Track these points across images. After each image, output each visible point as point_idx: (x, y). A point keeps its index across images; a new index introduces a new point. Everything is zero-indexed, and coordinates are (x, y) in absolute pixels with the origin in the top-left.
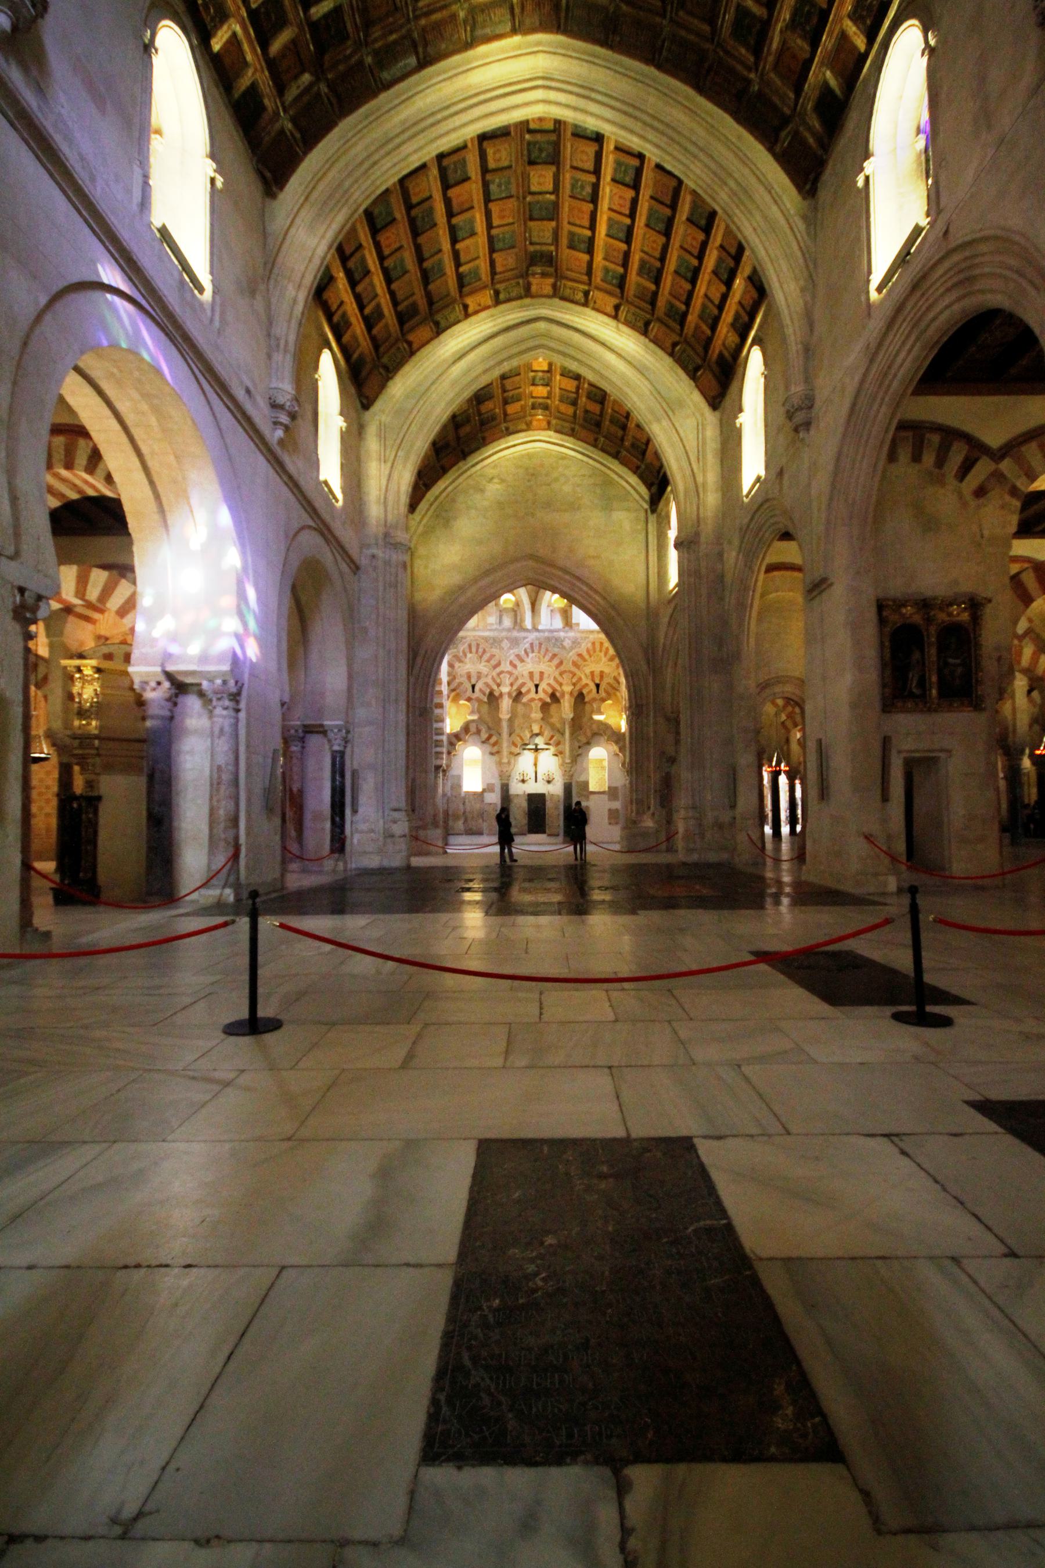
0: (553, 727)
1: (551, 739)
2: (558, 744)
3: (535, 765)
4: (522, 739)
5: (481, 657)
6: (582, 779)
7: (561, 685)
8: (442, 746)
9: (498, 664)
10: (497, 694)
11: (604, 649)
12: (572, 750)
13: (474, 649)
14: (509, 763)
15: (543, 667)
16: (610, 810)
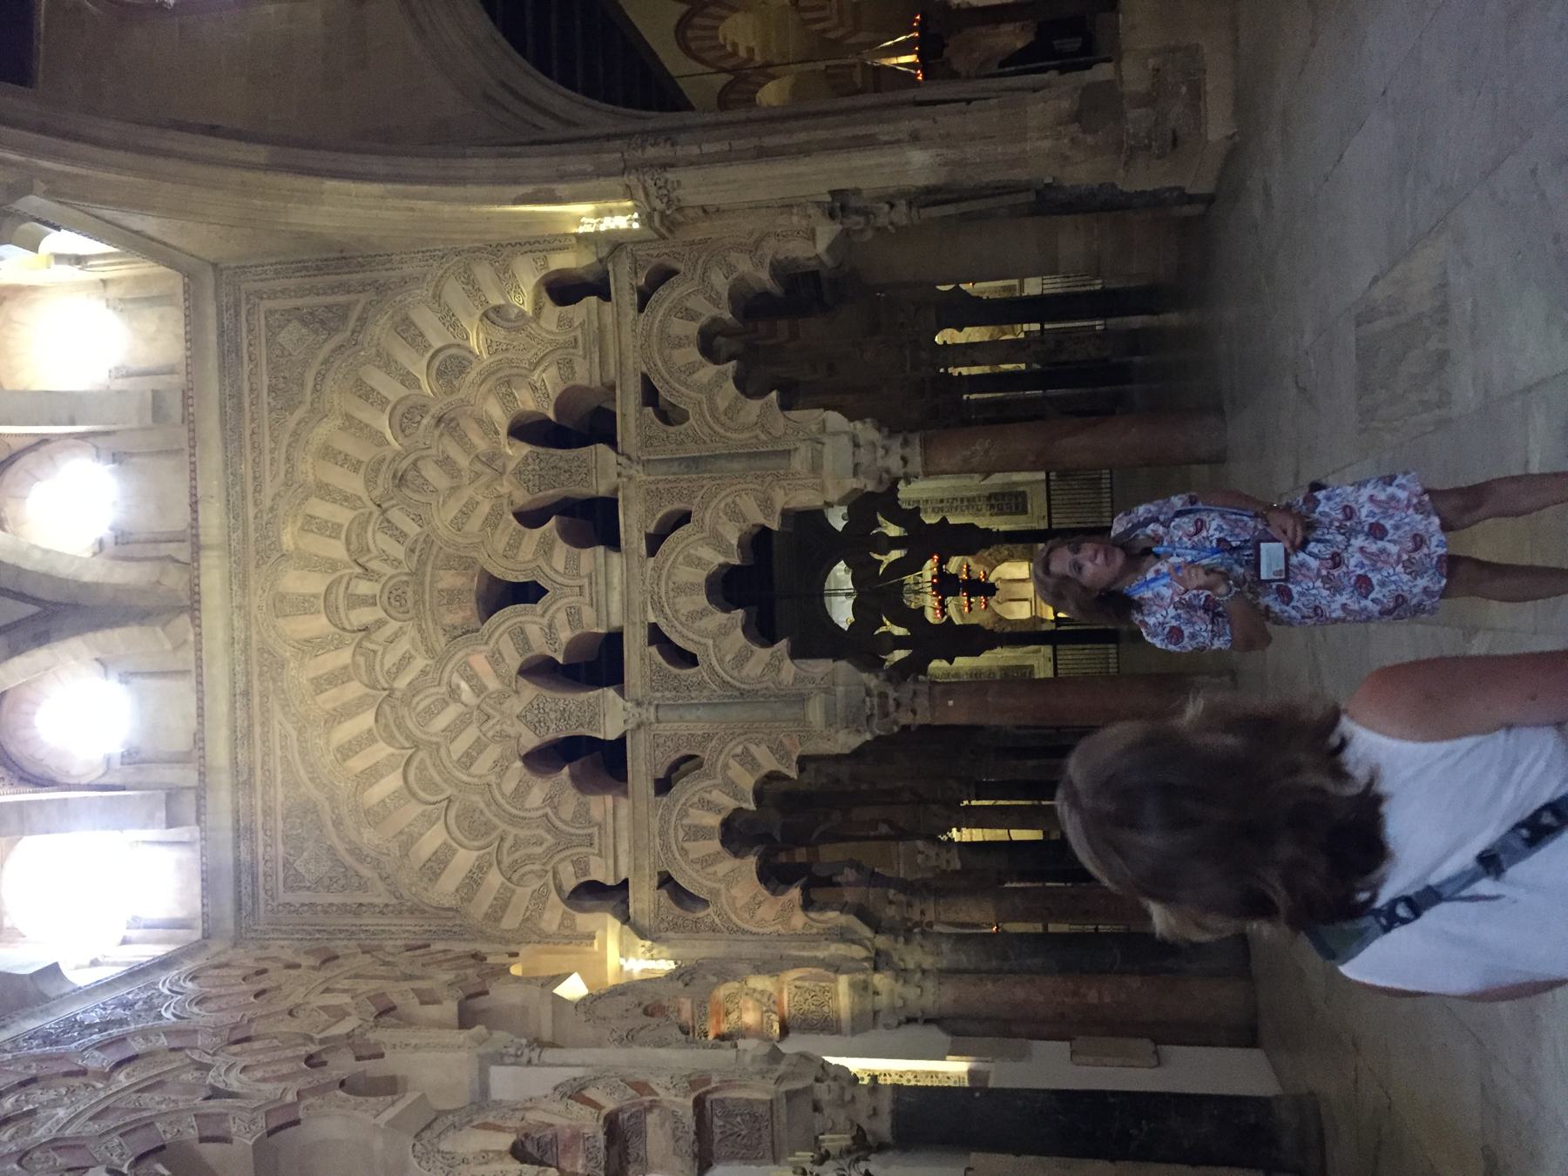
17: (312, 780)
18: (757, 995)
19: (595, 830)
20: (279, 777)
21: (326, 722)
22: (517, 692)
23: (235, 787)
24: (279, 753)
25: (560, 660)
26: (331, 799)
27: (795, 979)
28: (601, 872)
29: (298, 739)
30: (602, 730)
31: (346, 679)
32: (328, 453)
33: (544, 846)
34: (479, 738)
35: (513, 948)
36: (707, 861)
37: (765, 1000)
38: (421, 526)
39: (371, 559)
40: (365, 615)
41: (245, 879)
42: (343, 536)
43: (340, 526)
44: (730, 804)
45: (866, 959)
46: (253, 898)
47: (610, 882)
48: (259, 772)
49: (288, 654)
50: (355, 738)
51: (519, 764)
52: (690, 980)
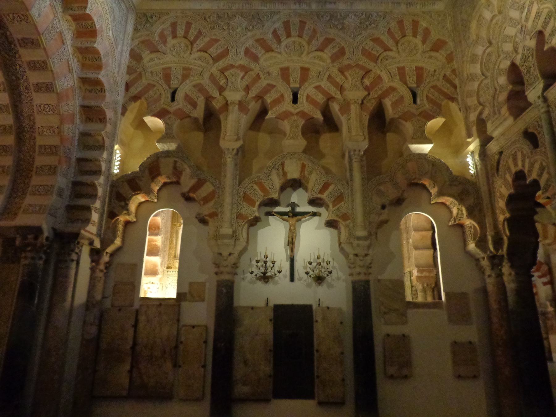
0: (327, 171)
1: (322, 191)
2: (339, 198)
3: (291, 243)
4: (263, 189)
5: (192, 44)
6: (388, 275)
7: (341, 89)
8: (94, 196)
9: (224, 54)
10: (217, 105)
11: (420, 31)
12: (366, 213)
13: (181, 32)
14: (234, 236)
15: (306, 60)
16: (455, 343)
18: (460, 212)
19: (498, 115)
22: (531, 39)
25: (546, 48)
27: (473, 225)
28: (490, 126)
30: (528, 92)
33: (489, 97)
34: (513, 36)
35: (461, 109)
36: (509, 169)
37: (459, 216)
44: (526, 171)
45: (491, 252)
47: (488, 133)
51: (508, 63)
52: (455, 185)
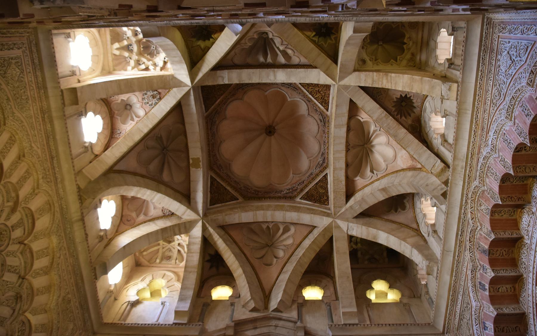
17: (22, 122)
20: (34, 120)
21: (24, 156)
23: (49, 110)
24: (36, 132)
26: (13, 113)
29: (31, 142)
31: (19, 182)
32: (48, 289)
38: (4, 281)
39: (18, 249)
40: (15, 218)
41: (36, 61)
42: (35, 255)
43: (37, 259)
46: (31, 51)
48: (41, 119)
49: (44, 185)
50: (9, 150)
